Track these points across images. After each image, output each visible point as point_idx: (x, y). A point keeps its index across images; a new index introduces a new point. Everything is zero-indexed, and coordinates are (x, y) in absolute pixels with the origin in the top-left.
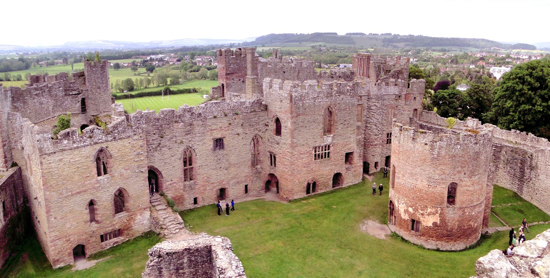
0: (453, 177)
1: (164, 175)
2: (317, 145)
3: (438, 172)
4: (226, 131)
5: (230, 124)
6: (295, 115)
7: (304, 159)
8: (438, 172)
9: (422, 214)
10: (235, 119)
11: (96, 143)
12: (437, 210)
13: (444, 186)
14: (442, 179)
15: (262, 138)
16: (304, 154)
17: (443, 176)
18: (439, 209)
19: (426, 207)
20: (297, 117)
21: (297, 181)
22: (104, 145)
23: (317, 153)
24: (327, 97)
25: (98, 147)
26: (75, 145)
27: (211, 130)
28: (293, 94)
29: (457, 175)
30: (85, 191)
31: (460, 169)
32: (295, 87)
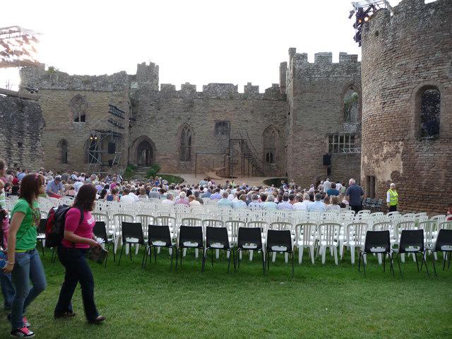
0: (424, 75)
1: (157, 148)
2: (333, 131)
3: (394, 73)
4: (231, 115)
5: (236, 108)
6: (300, 91)
7: (313, 149)
8: (394, 73)
9: (377, 161)
10: (244, 104)
11: (74, 90)
12: (397, 148)
13: (406, 96)
14: (403, 84)
15: (279, 131)
16: (312, 141)
17: (404, 79)
18: (401, 143)
19: (382, 146)
20: (301, 93)
21: (301, 175)
22: (82, 94)
23: (333, 143)
24: (348, 72)
25: (76, 94)
26: (53, 87)
27: (214, 111)
28: (297, 66)
29: (435, 70)
30: (58, 130)
31: (438, 55)
32: (299, 58)
